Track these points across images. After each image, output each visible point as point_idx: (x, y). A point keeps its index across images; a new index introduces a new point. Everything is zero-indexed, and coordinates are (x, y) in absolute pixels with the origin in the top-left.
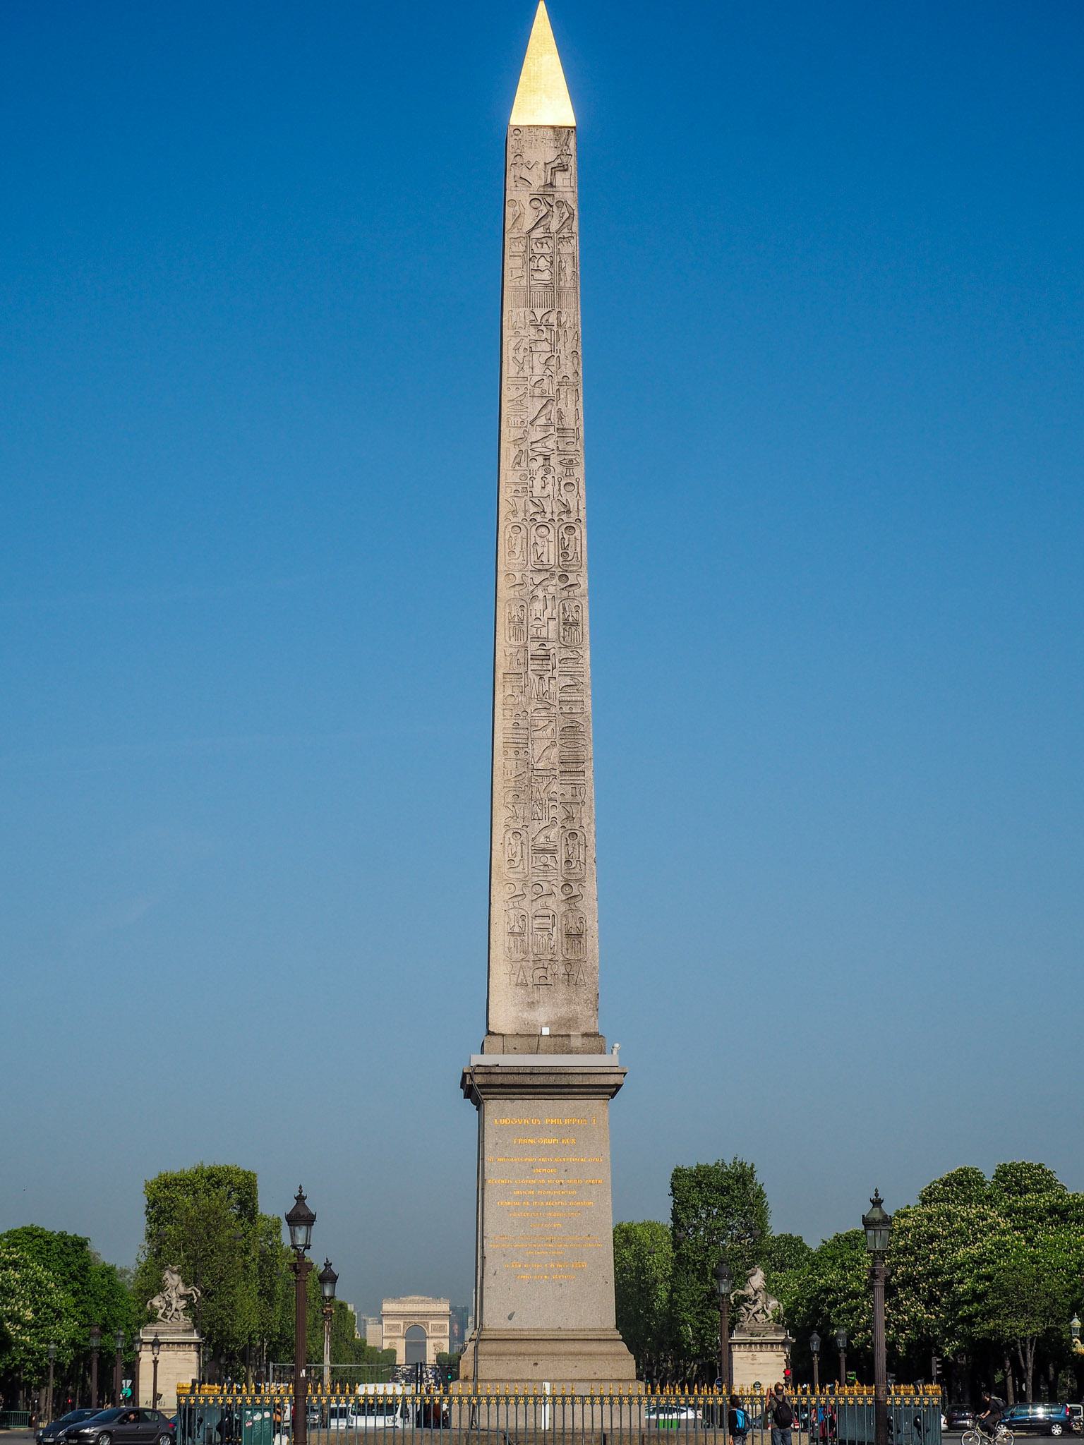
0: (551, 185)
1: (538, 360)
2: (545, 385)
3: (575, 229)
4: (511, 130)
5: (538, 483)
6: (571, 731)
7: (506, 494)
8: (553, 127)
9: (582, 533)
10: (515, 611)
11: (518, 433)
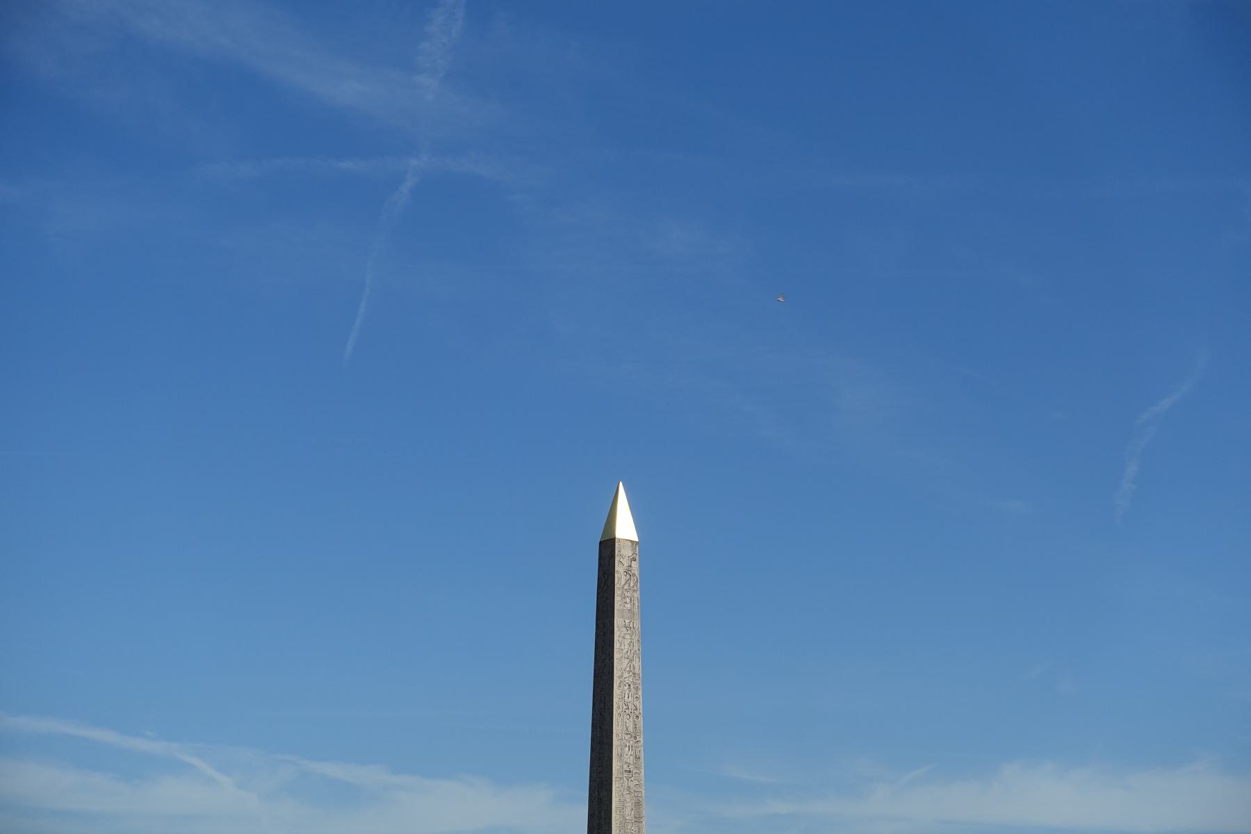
0: (631, 566)
1: (627, 642)
2: (629, 654)
3: (638, 587)
4: (616, 540)
5: (626, 696)
6: (638, 804)
7: (615, 700)
8: (631, 541)
9: (641, 719)
10: (620, 751)
11: (620, 673)
